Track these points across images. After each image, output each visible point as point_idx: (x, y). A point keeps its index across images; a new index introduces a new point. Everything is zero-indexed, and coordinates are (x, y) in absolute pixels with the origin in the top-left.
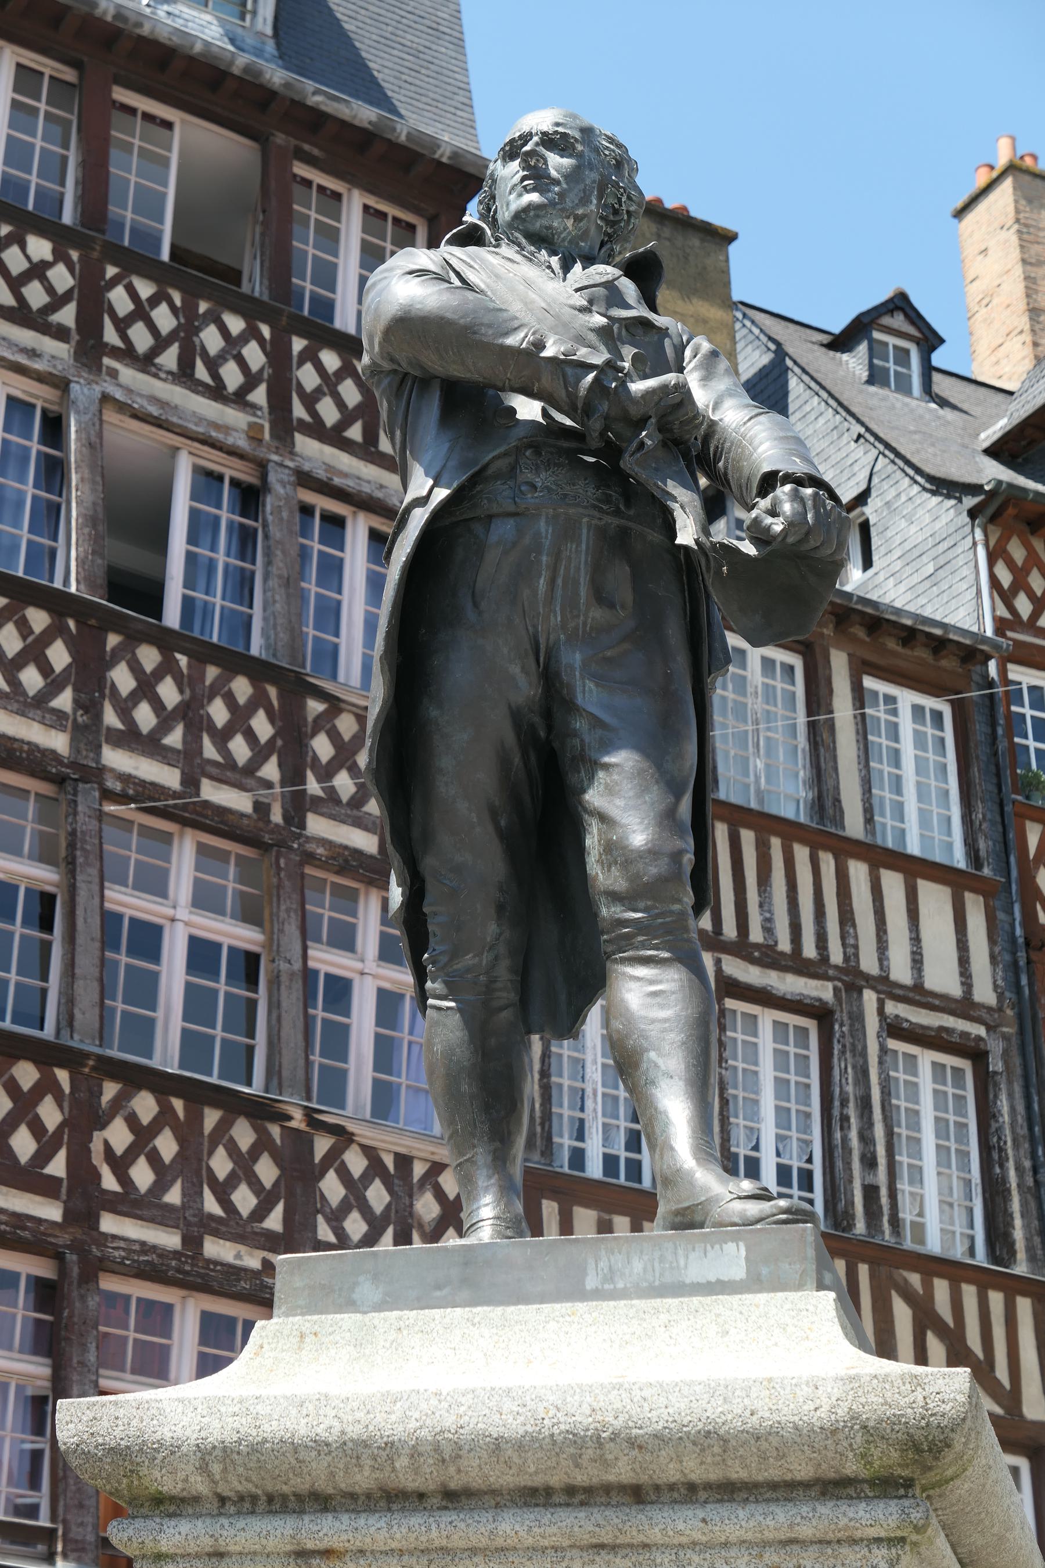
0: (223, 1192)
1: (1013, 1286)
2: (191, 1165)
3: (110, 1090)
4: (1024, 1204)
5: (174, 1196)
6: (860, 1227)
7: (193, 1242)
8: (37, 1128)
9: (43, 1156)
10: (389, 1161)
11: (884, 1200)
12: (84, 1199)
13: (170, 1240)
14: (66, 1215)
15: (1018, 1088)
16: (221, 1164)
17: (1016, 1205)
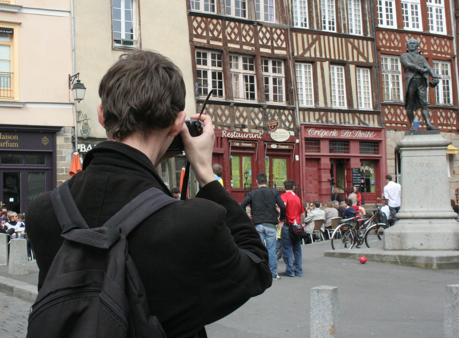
0: (245, 38)
1: (367, 39)
2: (240, 34)
3: (227, 22)
4: (370, 24)
5: (238, 39)
6: (343, 32)
7: (241, 47)
8: (217, 30)
9: (218, 35)
10: (269, 29)
11: (347, 26)
12: (225, 41)
13: (238, 47)
14: (223, 44)
15: (369, 3)
16: (244, 33)
17: (368, 25)
